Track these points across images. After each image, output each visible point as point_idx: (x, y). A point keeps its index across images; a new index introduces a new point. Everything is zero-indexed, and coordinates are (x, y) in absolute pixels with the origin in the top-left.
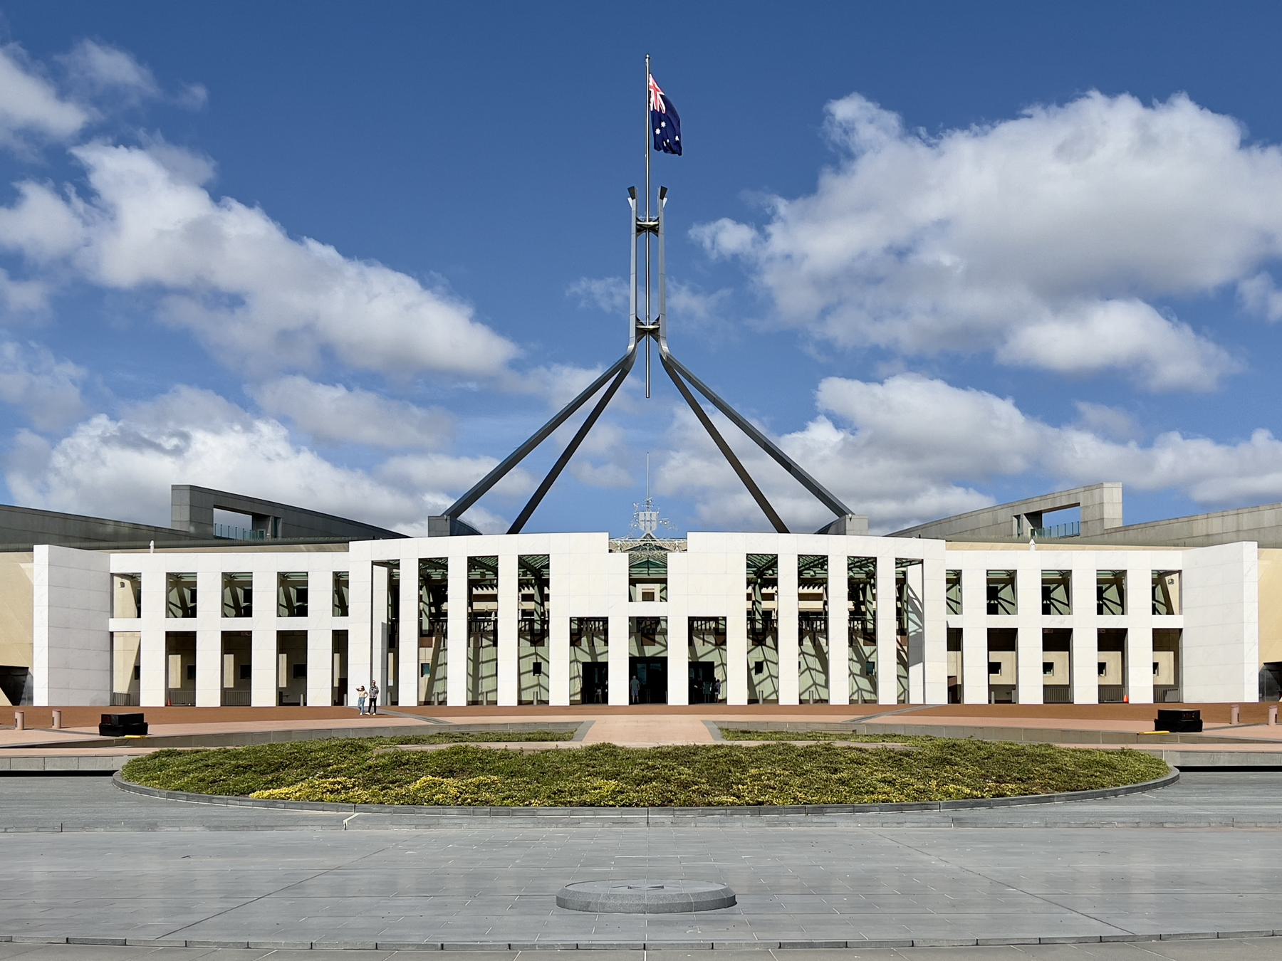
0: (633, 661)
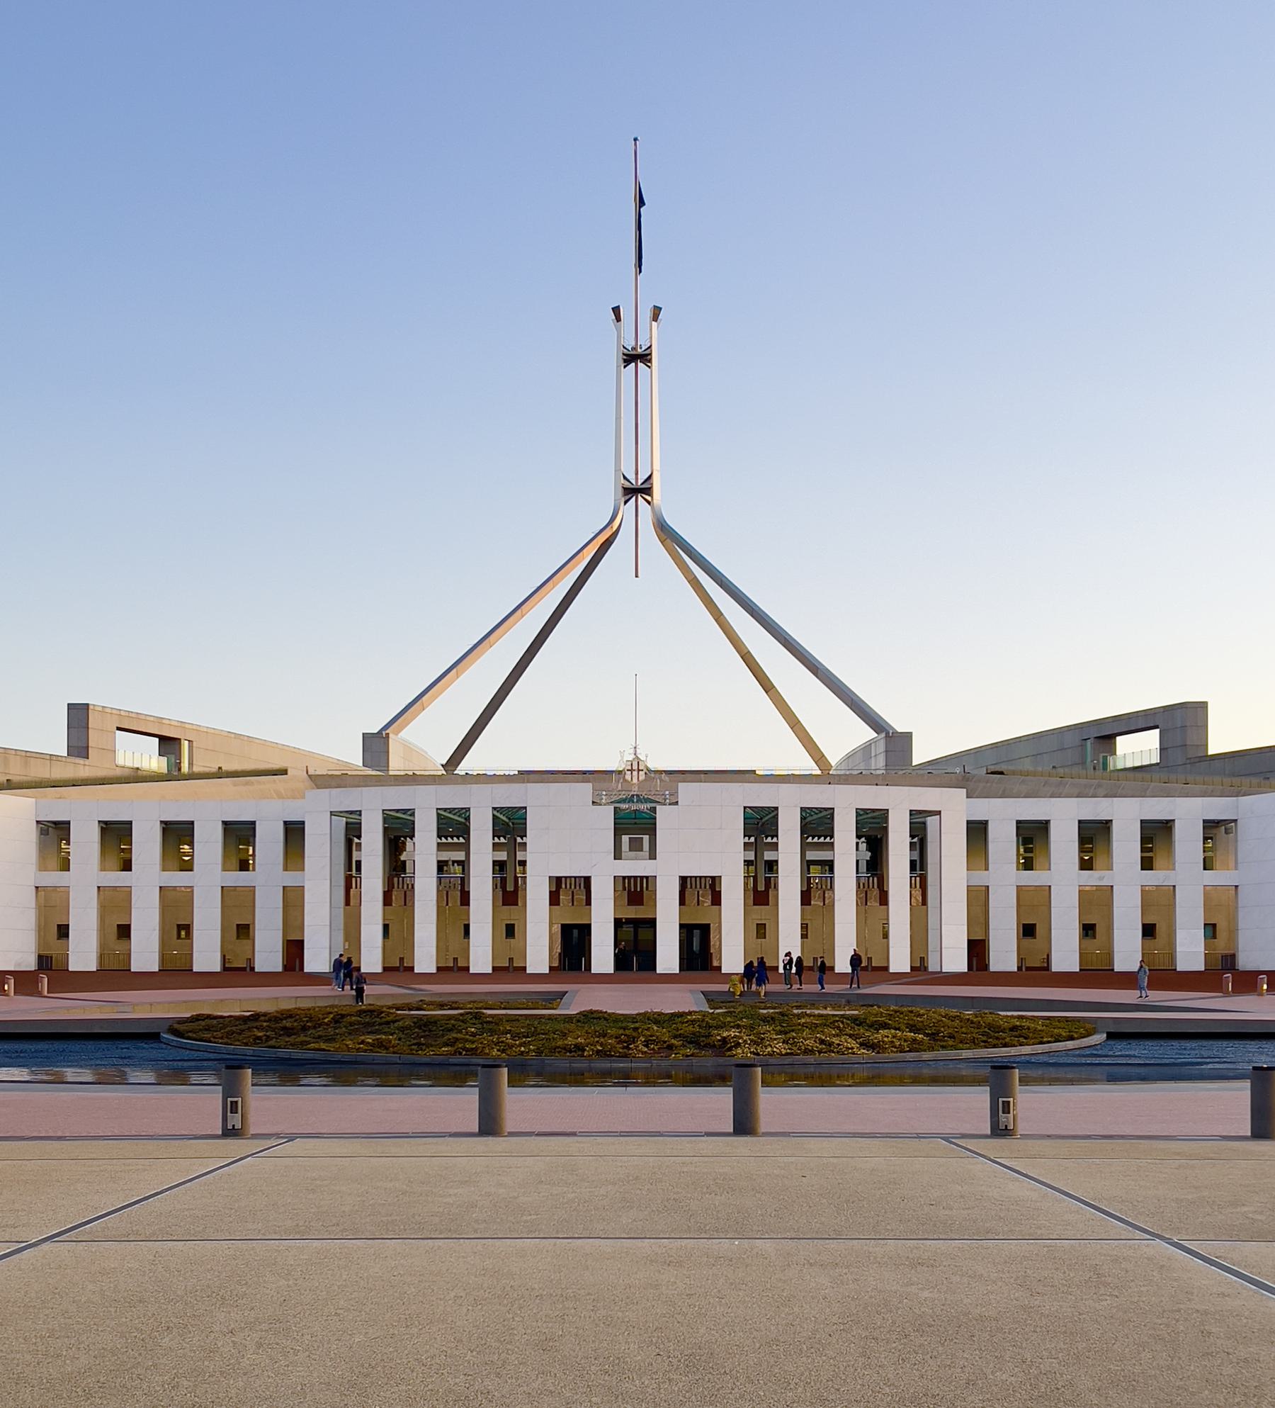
0: (618, 923)
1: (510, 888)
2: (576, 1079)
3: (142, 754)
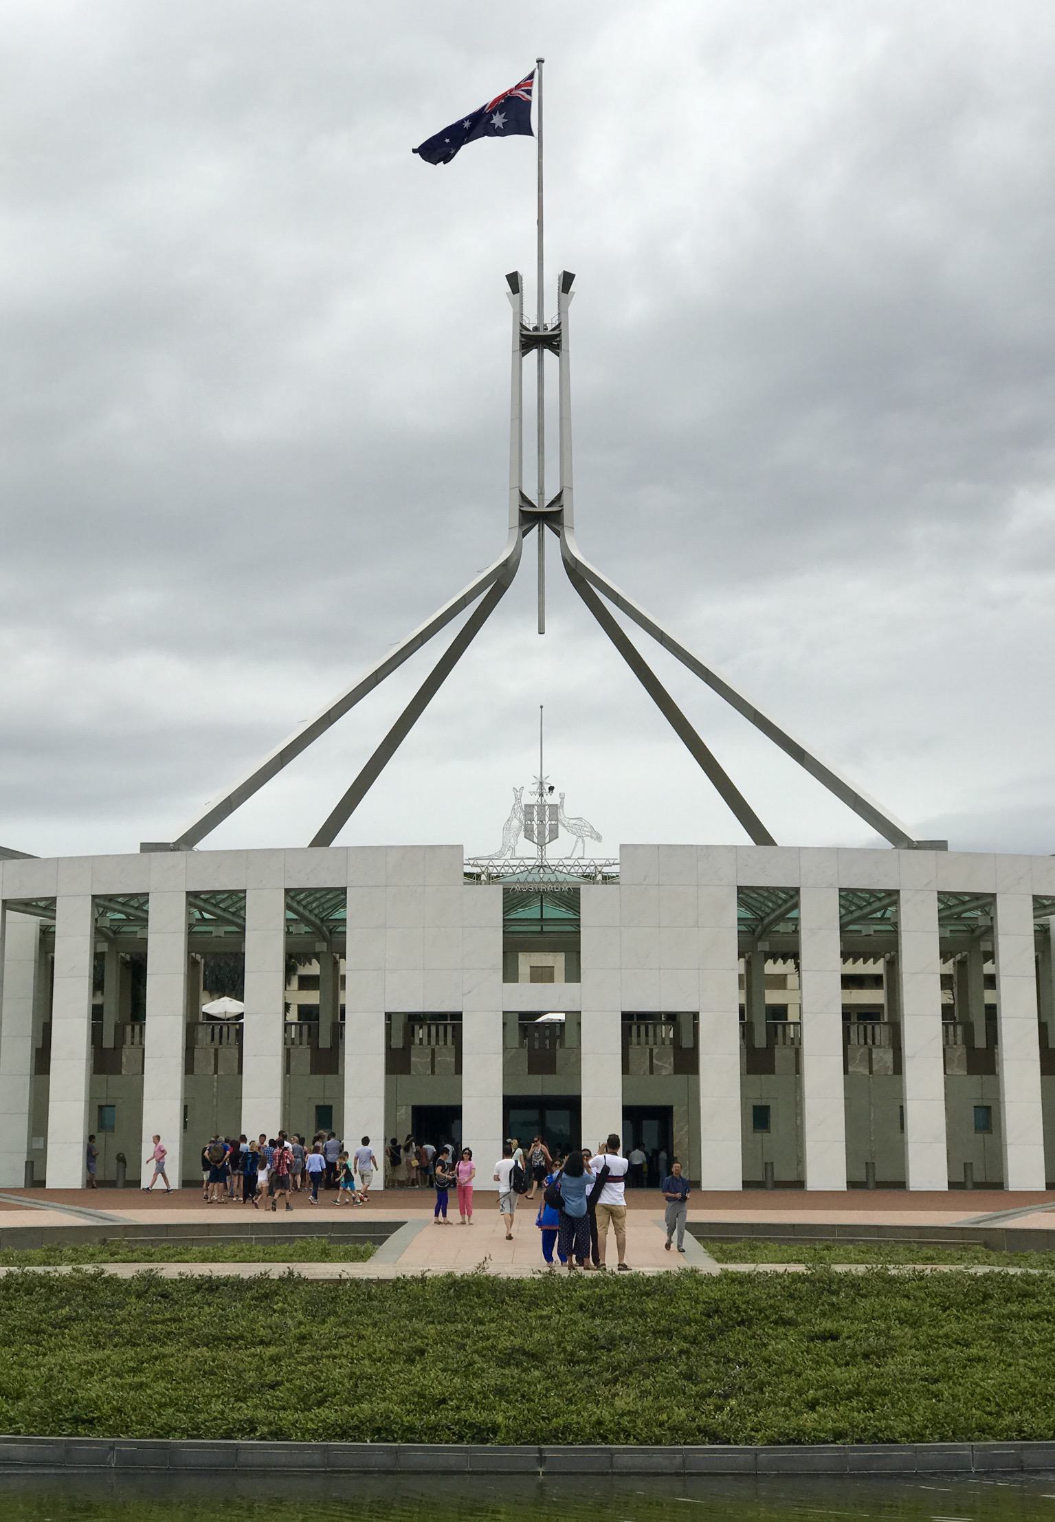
0: (510, 1104)
1: (325, 1042)
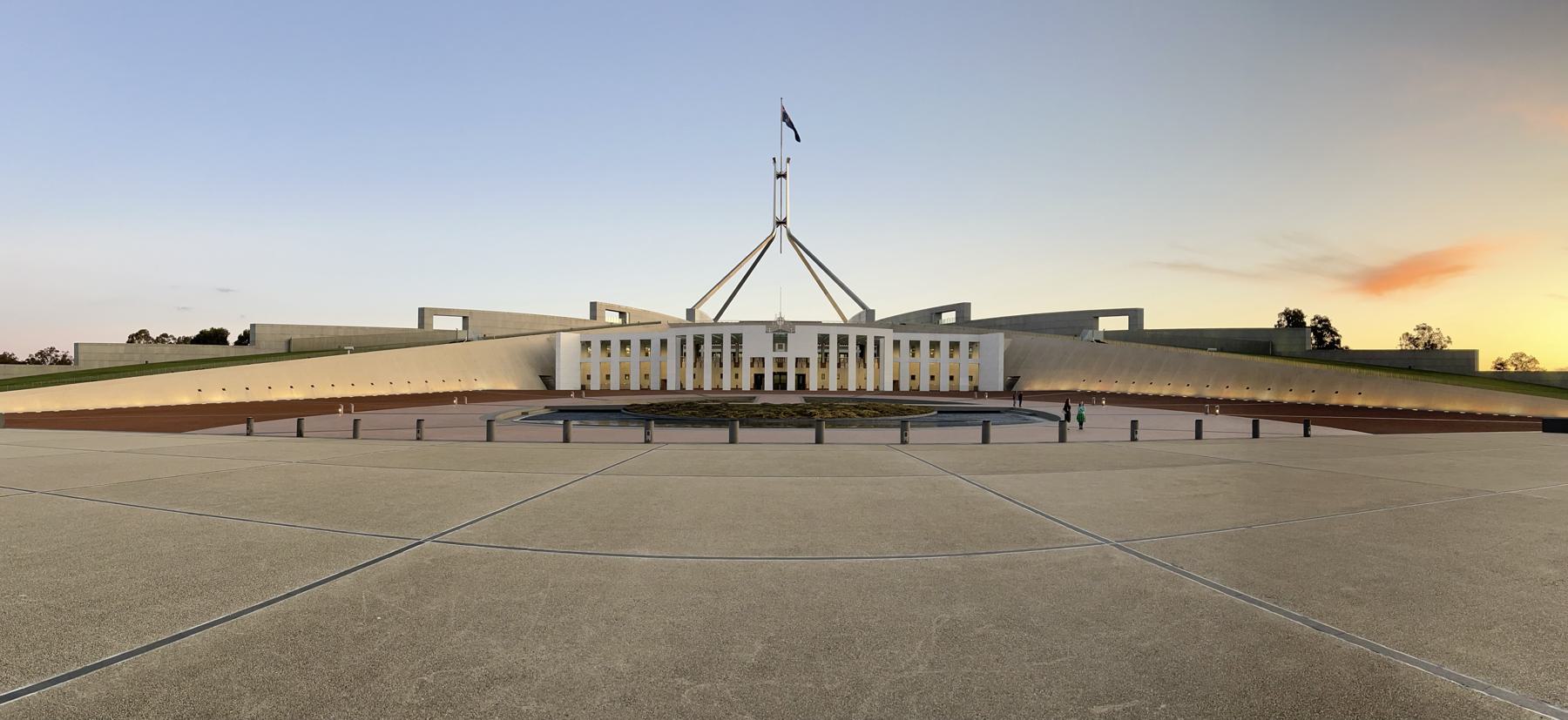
2: (760, 426)
3: (613, 318)
